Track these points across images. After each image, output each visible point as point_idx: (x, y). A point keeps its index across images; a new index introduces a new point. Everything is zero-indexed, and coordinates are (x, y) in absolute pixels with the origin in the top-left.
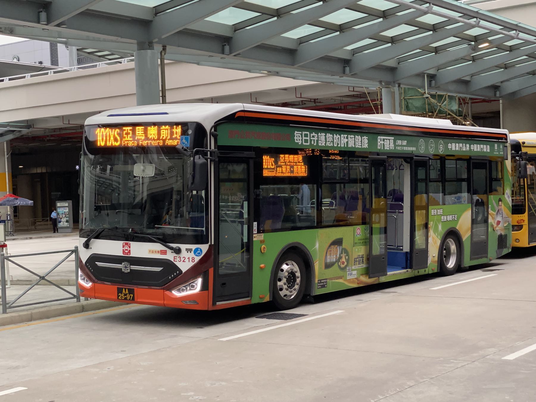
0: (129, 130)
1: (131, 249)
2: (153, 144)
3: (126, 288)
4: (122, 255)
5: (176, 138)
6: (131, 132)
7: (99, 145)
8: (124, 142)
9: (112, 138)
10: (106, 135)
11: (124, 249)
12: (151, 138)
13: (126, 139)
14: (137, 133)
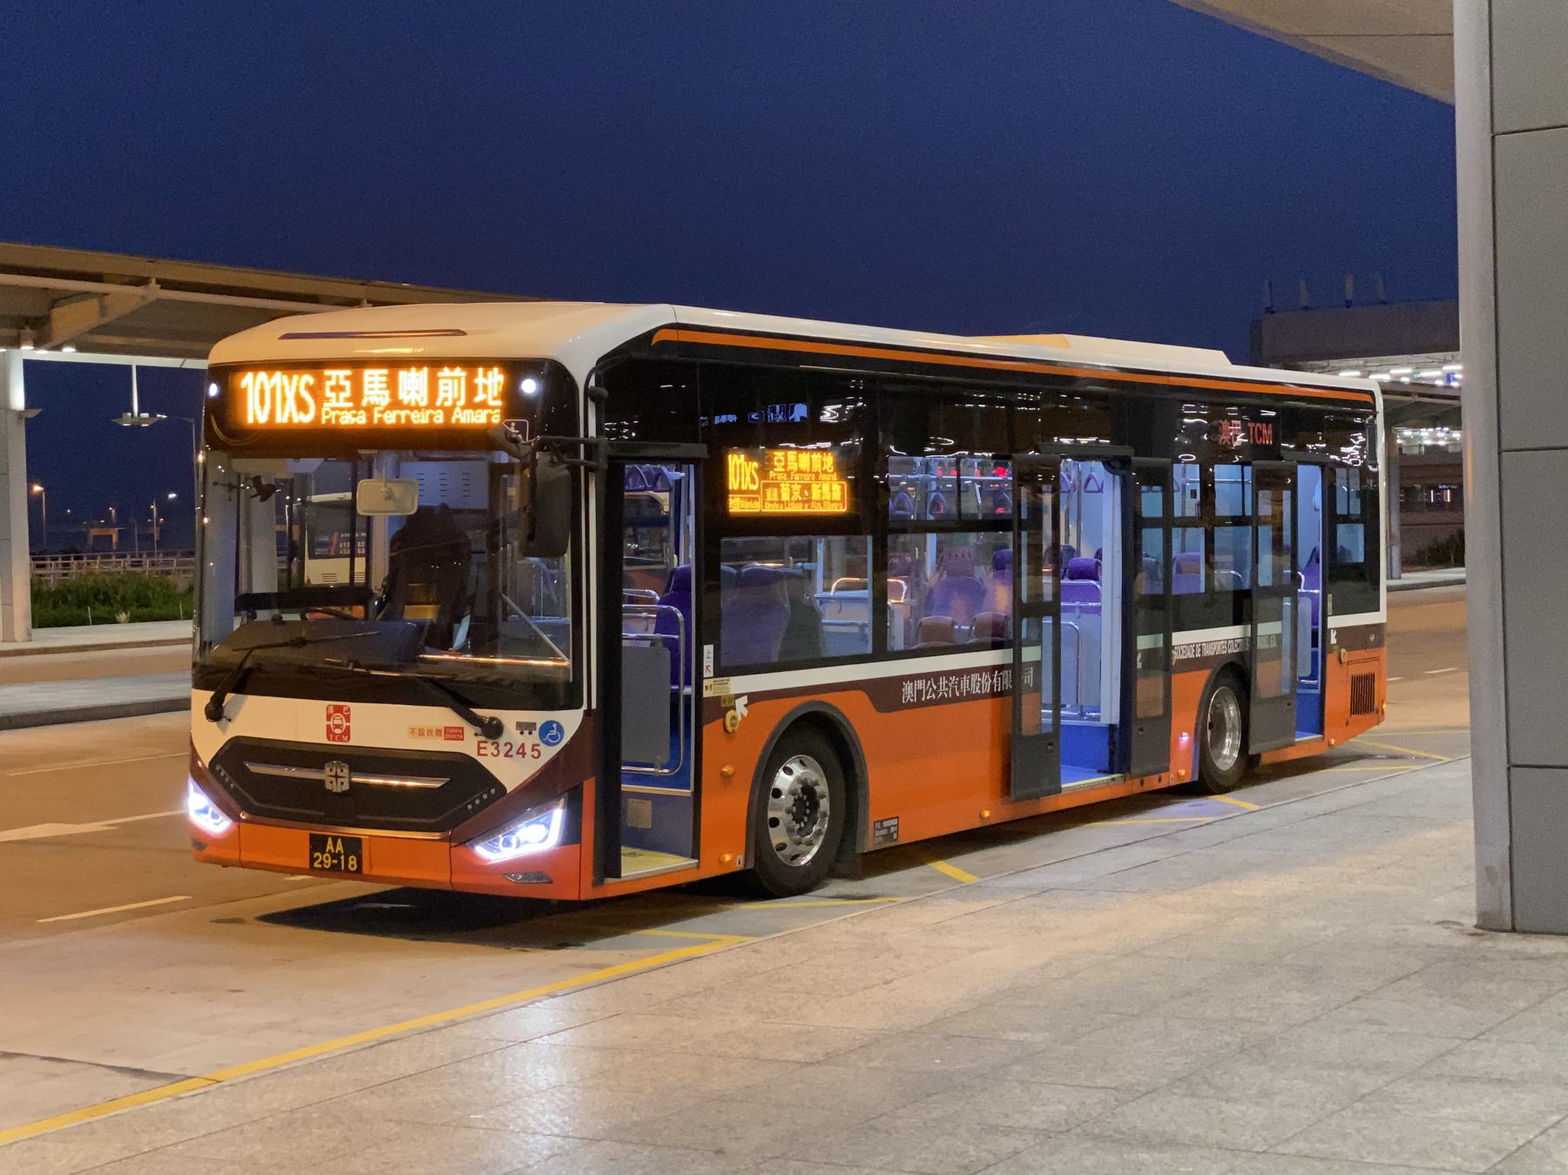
1: (352, 725)
2: (416, 419)
3: (339, 837)
5: (483, 405)
6: (347, 384)
7: (250, 420)
8: (327, 413)
9: (291, 404)
10: (273, 390)
11: (331, 723)
13: (334, 404)
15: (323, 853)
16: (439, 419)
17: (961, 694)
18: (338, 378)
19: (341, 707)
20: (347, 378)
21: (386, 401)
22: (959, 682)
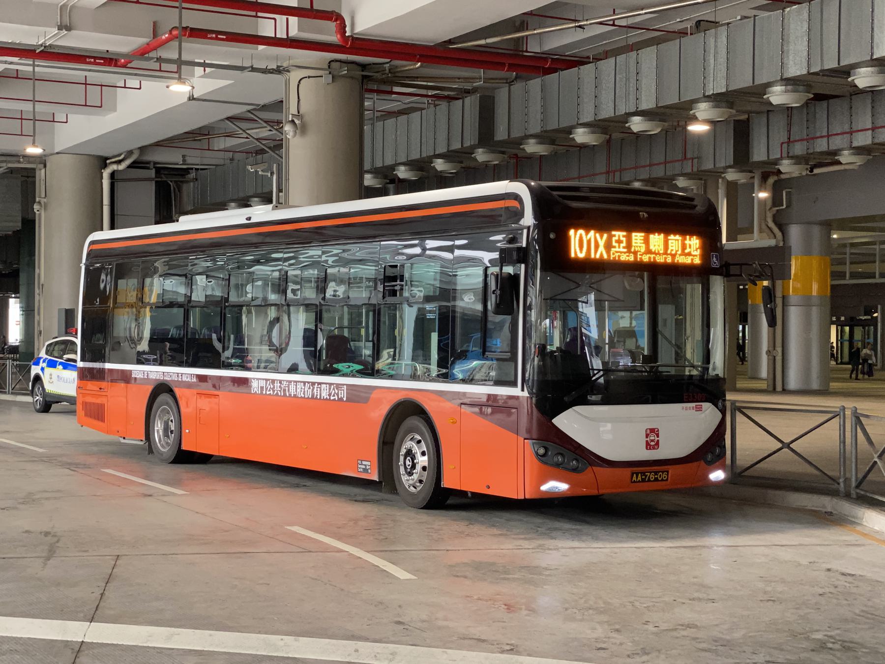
5: (689, 254)
6: (624, 239)
7: (573, 255)
8: (613, 254)
12: (655, 251)
13: (617, 249)
18: (619, 236)
20: (624, 236)
21: (643, 250)
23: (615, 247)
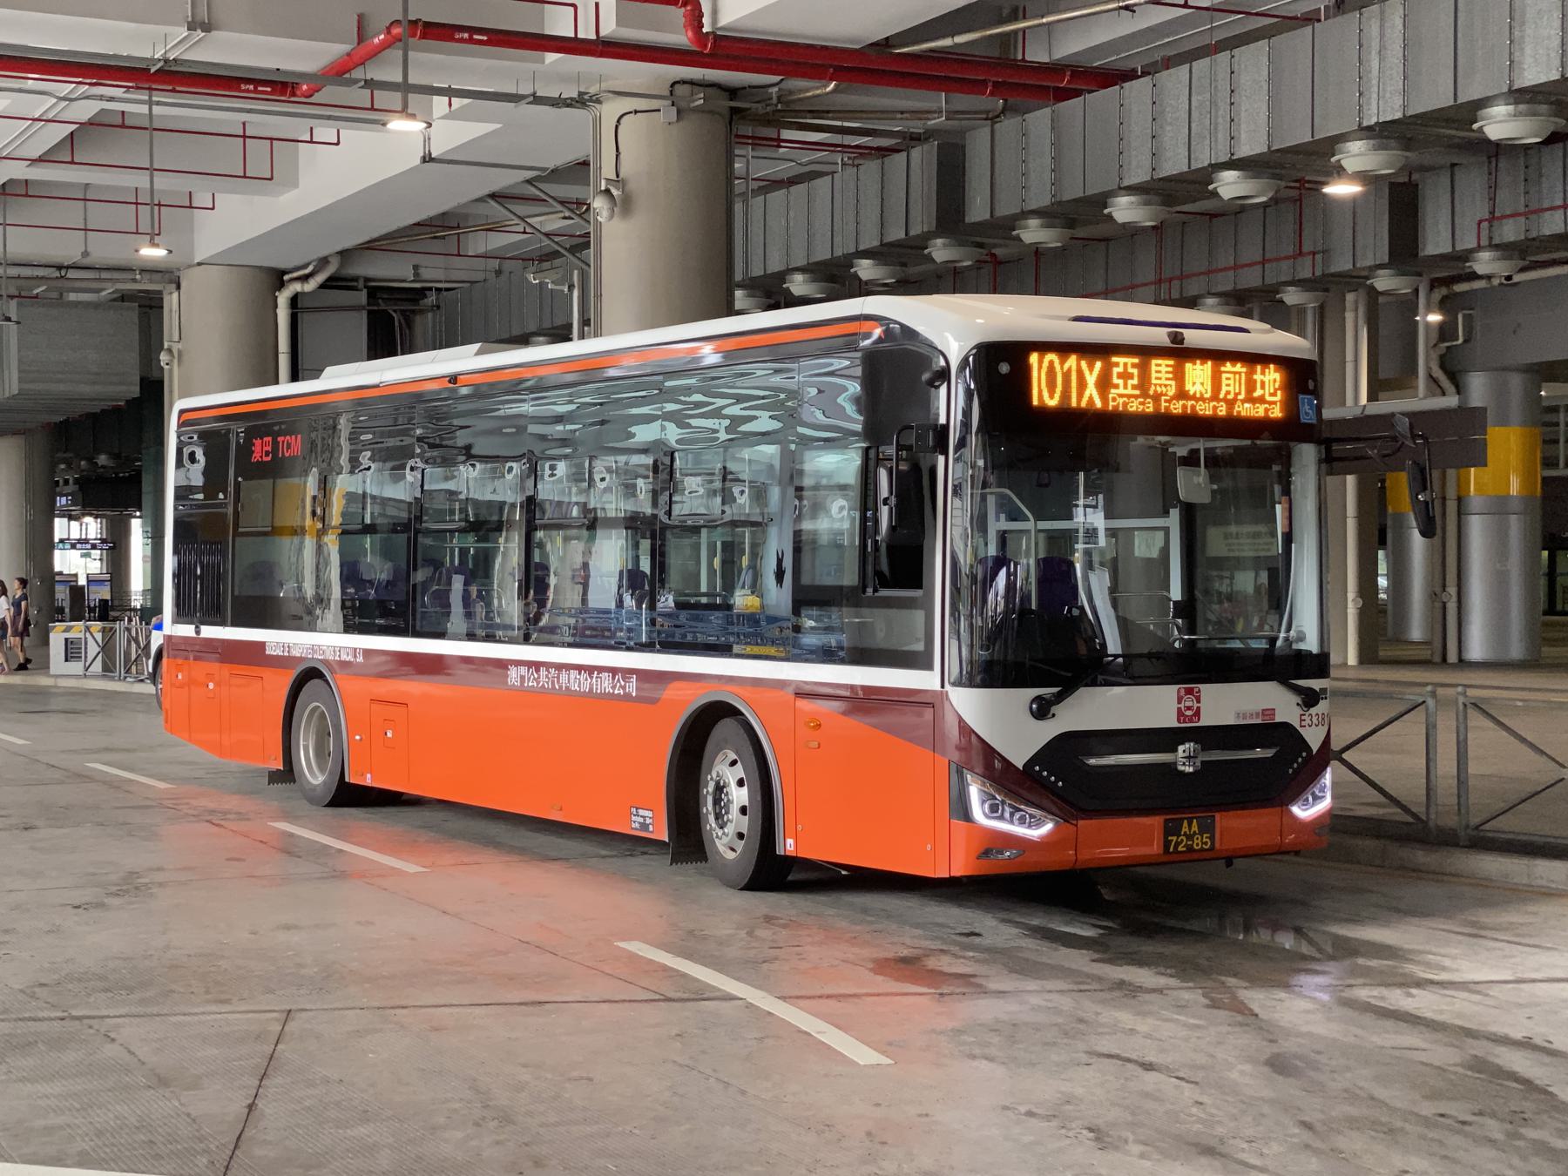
0: (1129, 366)
1: (1176, 705)
3: (1193, 818)
4: (1175, 724)
5: (1261, 400)
7: (1035, 402)
8: (1114, 399)
11: (1182, 706)
12: (1195, 393)
13: (1121, 391)
14: (1154, 375)
15: (1179, 835)
16: (1222, 411)
17: (561, 687)
18: (1125, 365)
19: (1192, 689)
20: (1134, 366)
21: (1172, 392)
22: (558, 674)
23: (1116, 386)
